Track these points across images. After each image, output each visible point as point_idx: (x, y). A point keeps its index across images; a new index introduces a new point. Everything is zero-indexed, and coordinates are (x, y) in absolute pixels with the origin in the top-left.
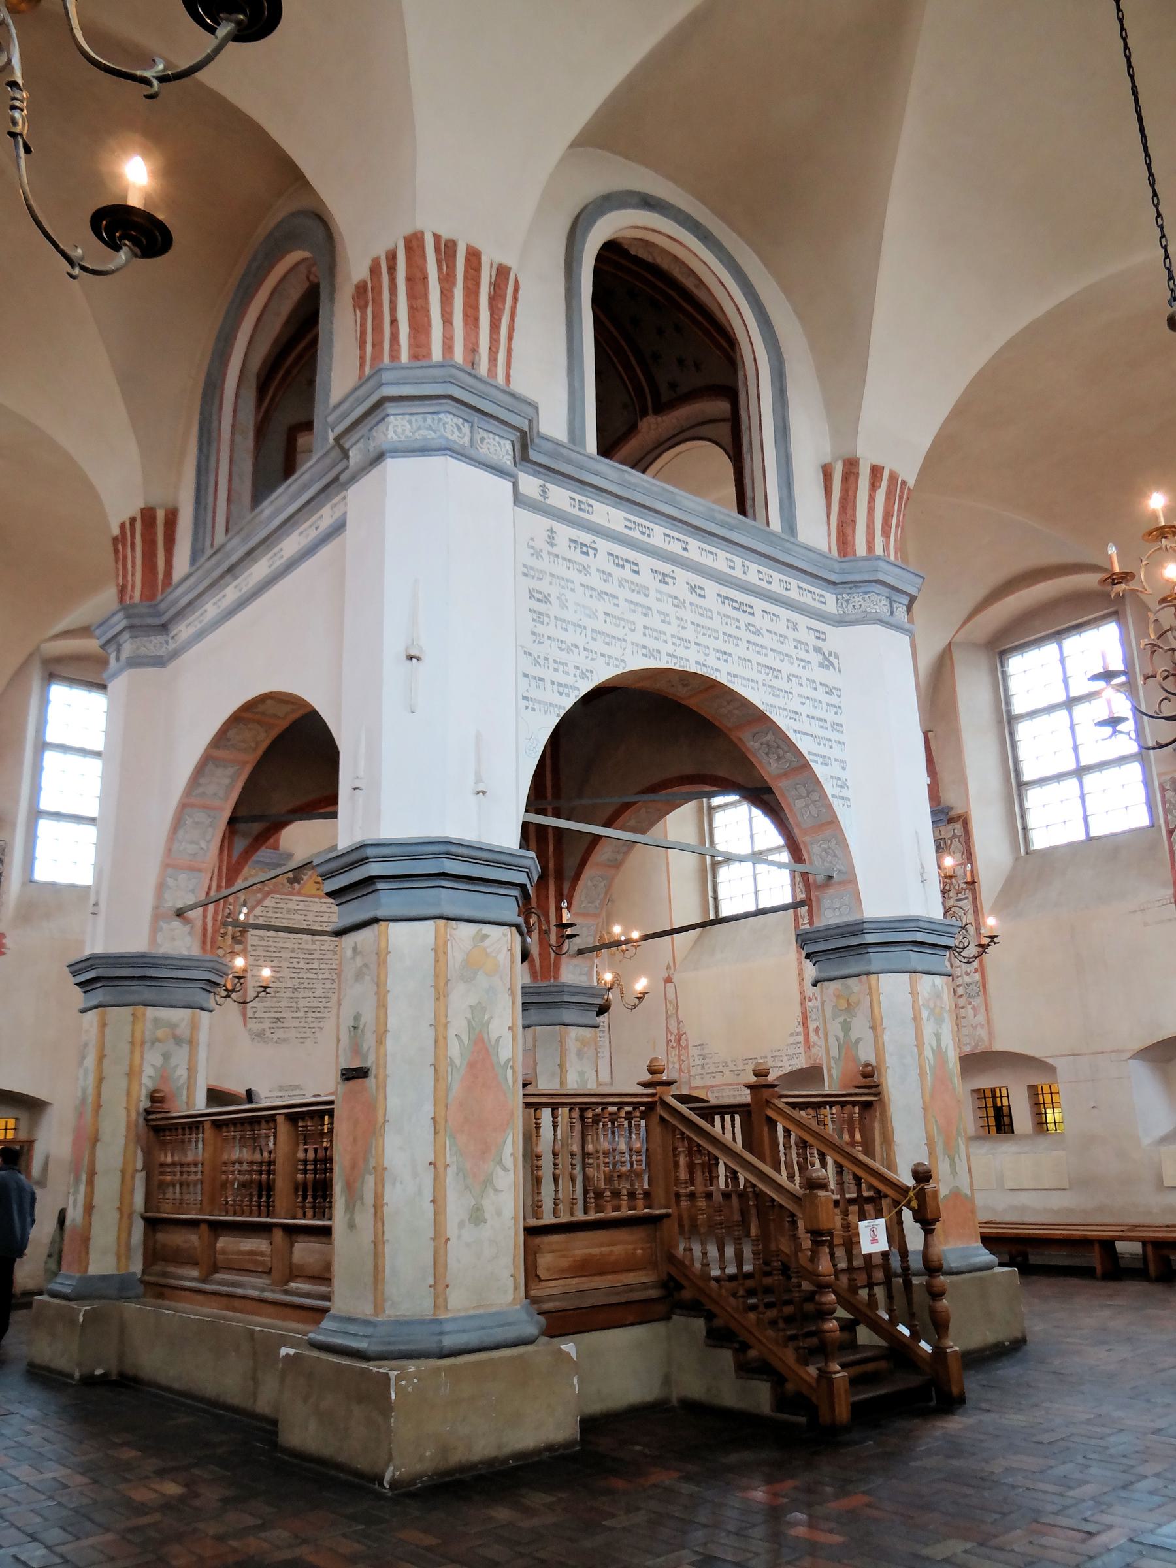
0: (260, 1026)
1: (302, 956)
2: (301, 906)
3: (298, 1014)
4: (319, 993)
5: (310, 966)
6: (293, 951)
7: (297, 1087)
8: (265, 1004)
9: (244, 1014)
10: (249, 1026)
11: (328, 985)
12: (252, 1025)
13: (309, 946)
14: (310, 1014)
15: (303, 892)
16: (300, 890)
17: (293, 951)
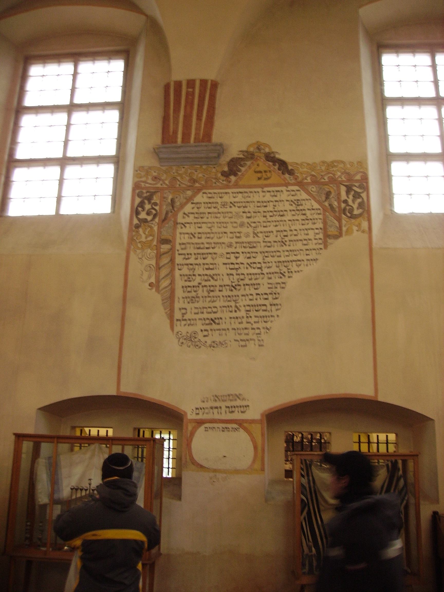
0: (191, 329)
1: (240, 250)
2: (240, 198)
3: (238, 314)
4: (263, 289)
5: (252, 260)
6: (230, 246)
7: (238, 397)
8: (196, 305)
9: (171, 317)
10: (180, 328)
11: (276, 279)
12: (180, 328)
13: (251, 239)
14: (252, 314)
15: (241, 183)
16: (236, 182)
17: (230, 246)
